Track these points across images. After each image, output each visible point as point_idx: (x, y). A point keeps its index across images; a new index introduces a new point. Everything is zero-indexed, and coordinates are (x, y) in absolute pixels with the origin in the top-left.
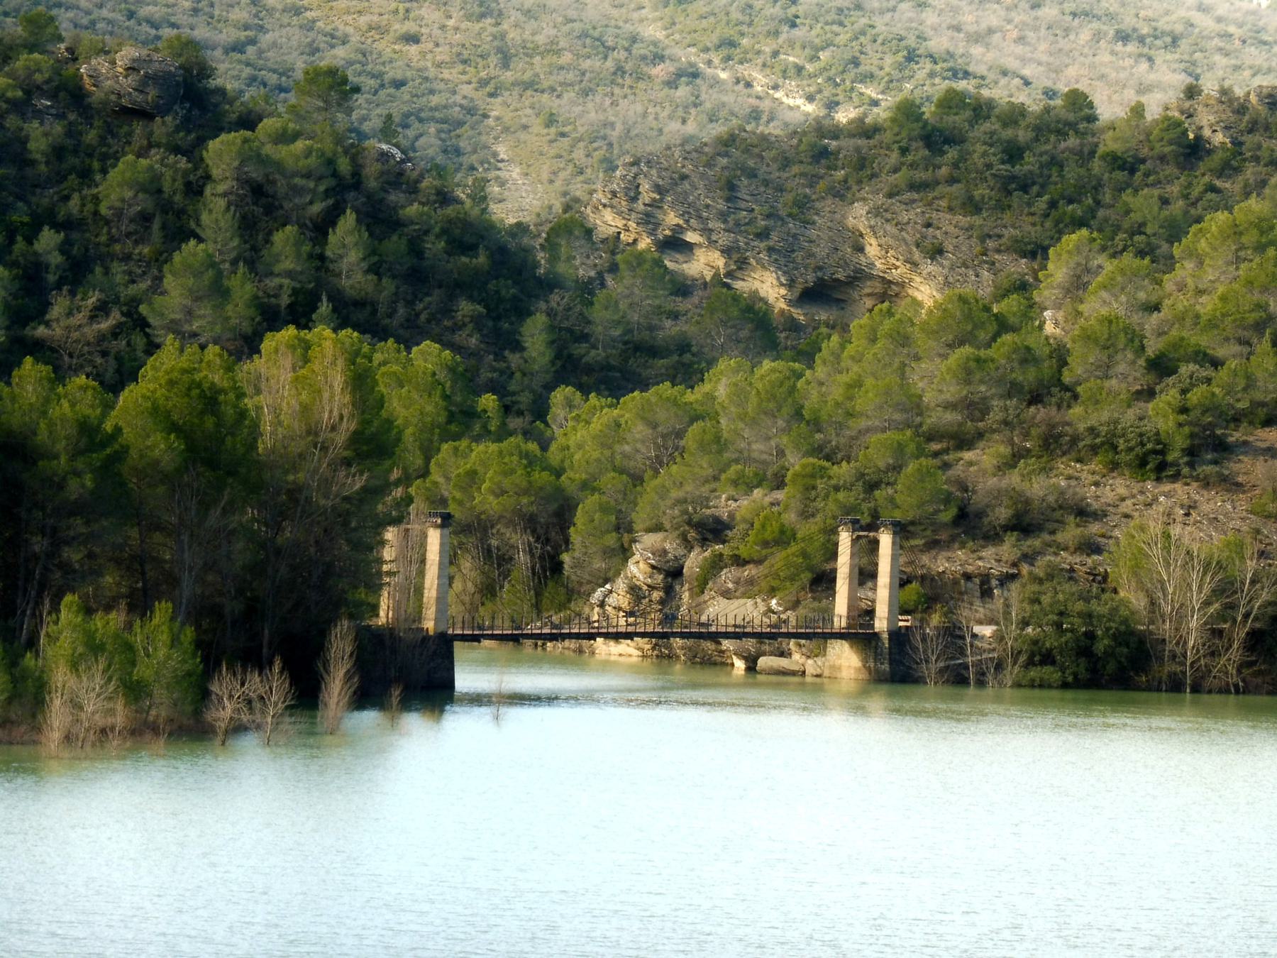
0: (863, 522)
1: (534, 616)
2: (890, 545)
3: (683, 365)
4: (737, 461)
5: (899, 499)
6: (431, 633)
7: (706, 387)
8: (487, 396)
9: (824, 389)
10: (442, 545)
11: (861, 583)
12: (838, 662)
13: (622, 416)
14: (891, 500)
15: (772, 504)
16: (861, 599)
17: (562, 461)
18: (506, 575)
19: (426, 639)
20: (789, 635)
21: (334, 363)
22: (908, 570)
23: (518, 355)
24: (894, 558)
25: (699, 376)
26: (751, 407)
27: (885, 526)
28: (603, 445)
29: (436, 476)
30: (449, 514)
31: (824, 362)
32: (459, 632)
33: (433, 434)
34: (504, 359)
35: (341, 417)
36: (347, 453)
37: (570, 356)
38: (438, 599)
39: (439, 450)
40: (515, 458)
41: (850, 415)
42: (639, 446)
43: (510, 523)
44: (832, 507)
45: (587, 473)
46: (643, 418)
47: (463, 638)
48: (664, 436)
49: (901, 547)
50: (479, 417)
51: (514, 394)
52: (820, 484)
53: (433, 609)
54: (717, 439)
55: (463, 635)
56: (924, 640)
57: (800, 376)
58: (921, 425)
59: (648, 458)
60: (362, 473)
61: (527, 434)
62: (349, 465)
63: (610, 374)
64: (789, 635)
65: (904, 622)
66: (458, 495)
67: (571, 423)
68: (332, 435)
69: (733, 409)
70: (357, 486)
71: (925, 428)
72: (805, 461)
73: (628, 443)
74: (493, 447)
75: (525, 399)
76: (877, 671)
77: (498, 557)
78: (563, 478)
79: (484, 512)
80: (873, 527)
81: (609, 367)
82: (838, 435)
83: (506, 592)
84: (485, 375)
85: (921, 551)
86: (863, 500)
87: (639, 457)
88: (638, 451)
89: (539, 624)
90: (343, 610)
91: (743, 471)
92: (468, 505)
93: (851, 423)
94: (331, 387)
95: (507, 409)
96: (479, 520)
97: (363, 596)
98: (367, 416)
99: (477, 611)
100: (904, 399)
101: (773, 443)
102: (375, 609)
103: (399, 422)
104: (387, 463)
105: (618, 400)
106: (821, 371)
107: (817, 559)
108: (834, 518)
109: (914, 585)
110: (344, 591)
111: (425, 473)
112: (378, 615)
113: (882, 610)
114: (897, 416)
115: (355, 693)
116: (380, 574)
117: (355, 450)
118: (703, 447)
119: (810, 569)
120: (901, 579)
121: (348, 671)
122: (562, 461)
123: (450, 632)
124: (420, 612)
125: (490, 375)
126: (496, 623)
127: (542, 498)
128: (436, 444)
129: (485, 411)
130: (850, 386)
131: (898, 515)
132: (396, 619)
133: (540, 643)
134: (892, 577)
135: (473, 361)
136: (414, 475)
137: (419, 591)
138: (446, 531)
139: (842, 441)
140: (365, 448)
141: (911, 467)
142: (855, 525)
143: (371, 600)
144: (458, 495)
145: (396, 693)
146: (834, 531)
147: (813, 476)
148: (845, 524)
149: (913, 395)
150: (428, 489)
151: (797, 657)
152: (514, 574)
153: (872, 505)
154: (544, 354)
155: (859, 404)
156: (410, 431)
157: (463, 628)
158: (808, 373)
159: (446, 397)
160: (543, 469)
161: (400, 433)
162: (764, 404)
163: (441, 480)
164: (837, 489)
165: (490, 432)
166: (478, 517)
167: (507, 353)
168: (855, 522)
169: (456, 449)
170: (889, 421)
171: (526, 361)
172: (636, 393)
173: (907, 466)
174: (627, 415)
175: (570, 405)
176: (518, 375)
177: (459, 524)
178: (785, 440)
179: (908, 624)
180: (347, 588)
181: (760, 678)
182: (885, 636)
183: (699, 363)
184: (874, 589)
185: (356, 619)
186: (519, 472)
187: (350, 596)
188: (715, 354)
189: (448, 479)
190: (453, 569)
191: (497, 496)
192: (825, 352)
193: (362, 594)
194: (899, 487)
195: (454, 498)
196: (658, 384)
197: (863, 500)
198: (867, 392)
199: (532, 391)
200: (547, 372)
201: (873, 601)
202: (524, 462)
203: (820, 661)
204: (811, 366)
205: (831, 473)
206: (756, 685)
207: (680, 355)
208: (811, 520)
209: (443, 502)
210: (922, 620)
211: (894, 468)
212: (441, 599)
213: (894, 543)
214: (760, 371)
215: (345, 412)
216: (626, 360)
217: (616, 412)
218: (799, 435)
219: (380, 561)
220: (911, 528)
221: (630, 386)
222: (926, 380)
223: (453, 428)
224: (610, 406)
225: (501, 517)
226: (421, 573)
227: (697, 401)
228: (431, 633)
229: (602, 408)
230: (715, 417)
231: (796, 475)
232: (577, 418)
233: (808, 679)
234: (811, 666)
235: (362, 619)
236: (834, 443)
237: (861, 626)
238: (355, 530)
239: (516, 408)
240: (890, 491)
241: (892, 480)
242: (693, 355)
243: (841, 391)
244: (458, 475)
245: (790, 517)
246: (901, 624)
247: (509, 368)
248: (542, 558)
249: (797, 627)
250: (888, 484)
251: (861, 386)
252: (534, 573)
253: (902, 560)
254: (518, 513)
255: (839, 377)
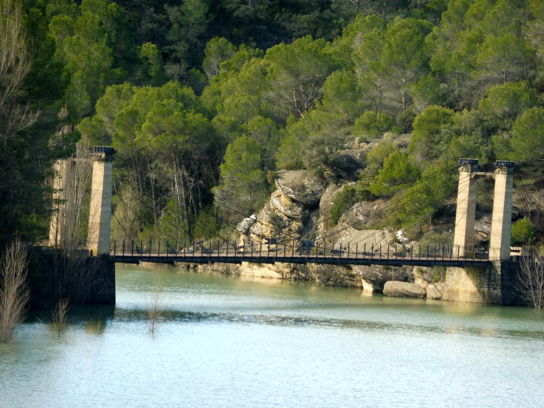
0: (481, 163)
1: (187, 241)
2: (504, 184)
3: (324, 20)
4: (369, 107)
5: (513, 143)
6: (95, 254)
7: (344, 41)
8: (147, 44)
9: (448, 44)
10: (105, 176)
11: (478, 218)
12: (456, 287)
13: (269, 65)
14: (507, 144)
15: (400, 146)
16: (477, 231)
17: (214, 105)
18: (163, 205)
19: (90, 259)
20: (413, 263)
21: (12, 11)
22: (520, 206)
23: (176, 8)
24: (508, 195)
25: (337, 30)
26: (383, 60)
27: (501, 167)
28: (251, 92)
29: (101, 115)
30: (112, 149)
31: (450, 20)
32: (120, 254)
33: (98, 77)
34: (163, 11)
35: (17, 61)
36: (21, 93)
37: (223, 10)
38: (101, 224)
39: (104, 92)
40: (172, 101)
41: (471, 67)
42: (282, 92)
43: (167, 159)
44: (453, 149)
45: (236, 116)
46: (287, 68)
47: (124, 260)
48: (305, 84)
49: (515, 186)
50: (141, 64)
51: (171, 43)
52: (444, 129)
53: (97, 233)
54: (353, 87)
55: (123, 257)
56: (532, 268)
57: (427, 31)
58: (534, 77)
59: (291, 104)
60: (34, 112)
61: (183, 80)
62: (24, 103)
63: (259, 27)
64: (413, 263)
65: (515, 253)
66: (121, 133)
67: (222, 71)
68: (8, 76)
69: (367, 60)
70: (31, 123)
71: (537, 80)
72: (430, 108)
73: (272, 90)
74: (152, 91)
75: (181, 48)
76: (490, 295)
77: (156, 189)
78: (215, 120)
79: (143, 149)
80: (489, 168)
81: (258, 21)
82: (460, 85)
83: (162, 220)
84: (147, 25)
85: (532, 190)
86: (482, 144)
87: (282, 102)
88: (281, 97)
89: (191, 249)
90: (16, 232)
91: (375, 116)
92: (129, 142)
93: (472, 74)
94: (9, 33)
95: (165, 57)
96: (140, 155)
97: (35, 220)
98: (39, 60)
99: (136, 236)
100: (520, 54)
101: (402, 92)
102: (45, 233)
103: (69, 66)
104: (58, 102)
105: (265, 50)
106: (446, 27)
107: (439, 195)
108: (455, 159)
109: (525, 220)
110: (17, 216)
111: (91, 113)
112: (47, 238)
113: (496, 242)
114: (514, 69)
115: (26, 306)
116: (50, 201)
117: (28, 90)
118: (339, 94)
119: (432, 204)
120: (513, 214)
121: (21, 287)
122: (214, 105)
123: (112, 254)
124: (86, 236)
125: (150, 26)
126: (153, 247)
127: (196, 137)
128: (101, 87)
129: (147, 58)
130: (472, 42)
131: (512, 158)
132: (64, 242)
133: (192, 265)
134: (505, 212)
135: (135, 13)
136: (82, 114)
137: (85, 217)
138: (110, 165)
139: (464, 90)
140: (37, 88)
141: (525, 115)
142: (474, 166)
143: (42, 224)
144: (121, 133)
145: (63, 307)
146: (455, 171)
147: (437, 122)
148: (465, 165)
149: (528, 51)
150: (93, 127)
151: (419, 281)
152: (170, 204)
153: (489, 148)
154: (198, 8)
155: (480, 58)
156: (78, 74)
157: (124, 251)
158: (435, 29)
159: (110, 44)
160: (197, 112)
161: (69, 76)
162: (395, 56)
163: (105, 119)
164: (458, 133)
165: (150, 77)
166: (138, 152)
167: (166, 6)
168: (473, 163)
169: (119, 91)
170: (507, 73)
171: (183, 14)
172: (281, 45)
173: (521, 114)
174: (272, 65)
175: (223, 55)
176: (176, 26)
177: (121, 158)
178: (413, 89)
179: (519, 254)
180: (20, 213)
181: (386, 300)
182: (498, 264)
183: (337, 19)
184: (489, 223)
185: (28, 241)
186: (176, 113)
187: (22, 220)
188: (354, 10)
189: (112, 118)
190: (115, 199)
191: (156, 135)
192: (450, 11)
193: (34, 219)
194: (514, 132)
195: (117, 136)
196: (301, 37)
197: (482, 144)
198: (487, 47)
199: (188, 41)
200: (201, 24)
201: (488, 234)
202: (181, 104)
203: (439, 286)
204: (436, 23)
205: (454, 119)
206: (384, 306)
207: (321, 11)
208: (435, 161)
209: (108, 138)
210: (531, 251)
211: (510, 116)
212: (104, 225)
213: (508, 183)
214: (391, 28)
215: (21, 57)
216: (272, 15)
217: (263, 62)
218: (426, 85)
219: (51, 190)
220: (524, 169)
221: (276, 38)
222: (539, 38)
223: (118, 71)
224: (257, 56)
225: (158, 154)
226: (87, 201)
227: (335, 53)
228: (95, 254)
229: (250, 57)
230: (351, 67)
231: (422, 120)
232: (228, 67)
233: (429, 302)
234: (431, 290)
235: (34, 241)
236: (456, 92)
237: (477, 256)
238: (29, 161)
239: (174, 55)
240: (506, 136)
241: (507, 126)
242: (332, 11)
243: (464, 45)
244: (121, 115)
245: (416, 158)
246: (512, 254)
247: (167, 19)
248: (195, 190)
249: (420, 255)
250: (504, 129)
251: (482, 41)
252: (187, 204)
253: (515, 197)
254: (174, 149)
255: (462, 33)
